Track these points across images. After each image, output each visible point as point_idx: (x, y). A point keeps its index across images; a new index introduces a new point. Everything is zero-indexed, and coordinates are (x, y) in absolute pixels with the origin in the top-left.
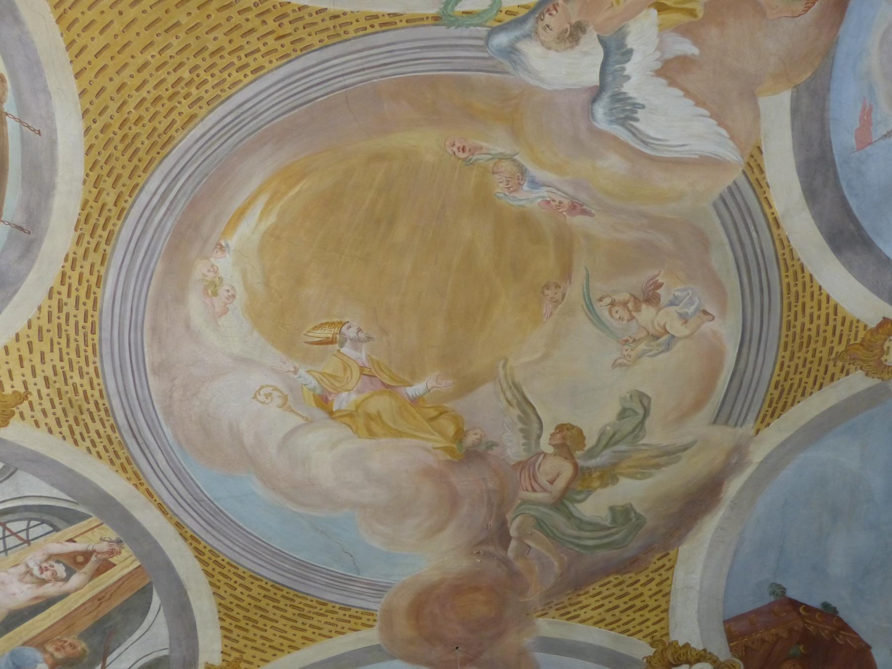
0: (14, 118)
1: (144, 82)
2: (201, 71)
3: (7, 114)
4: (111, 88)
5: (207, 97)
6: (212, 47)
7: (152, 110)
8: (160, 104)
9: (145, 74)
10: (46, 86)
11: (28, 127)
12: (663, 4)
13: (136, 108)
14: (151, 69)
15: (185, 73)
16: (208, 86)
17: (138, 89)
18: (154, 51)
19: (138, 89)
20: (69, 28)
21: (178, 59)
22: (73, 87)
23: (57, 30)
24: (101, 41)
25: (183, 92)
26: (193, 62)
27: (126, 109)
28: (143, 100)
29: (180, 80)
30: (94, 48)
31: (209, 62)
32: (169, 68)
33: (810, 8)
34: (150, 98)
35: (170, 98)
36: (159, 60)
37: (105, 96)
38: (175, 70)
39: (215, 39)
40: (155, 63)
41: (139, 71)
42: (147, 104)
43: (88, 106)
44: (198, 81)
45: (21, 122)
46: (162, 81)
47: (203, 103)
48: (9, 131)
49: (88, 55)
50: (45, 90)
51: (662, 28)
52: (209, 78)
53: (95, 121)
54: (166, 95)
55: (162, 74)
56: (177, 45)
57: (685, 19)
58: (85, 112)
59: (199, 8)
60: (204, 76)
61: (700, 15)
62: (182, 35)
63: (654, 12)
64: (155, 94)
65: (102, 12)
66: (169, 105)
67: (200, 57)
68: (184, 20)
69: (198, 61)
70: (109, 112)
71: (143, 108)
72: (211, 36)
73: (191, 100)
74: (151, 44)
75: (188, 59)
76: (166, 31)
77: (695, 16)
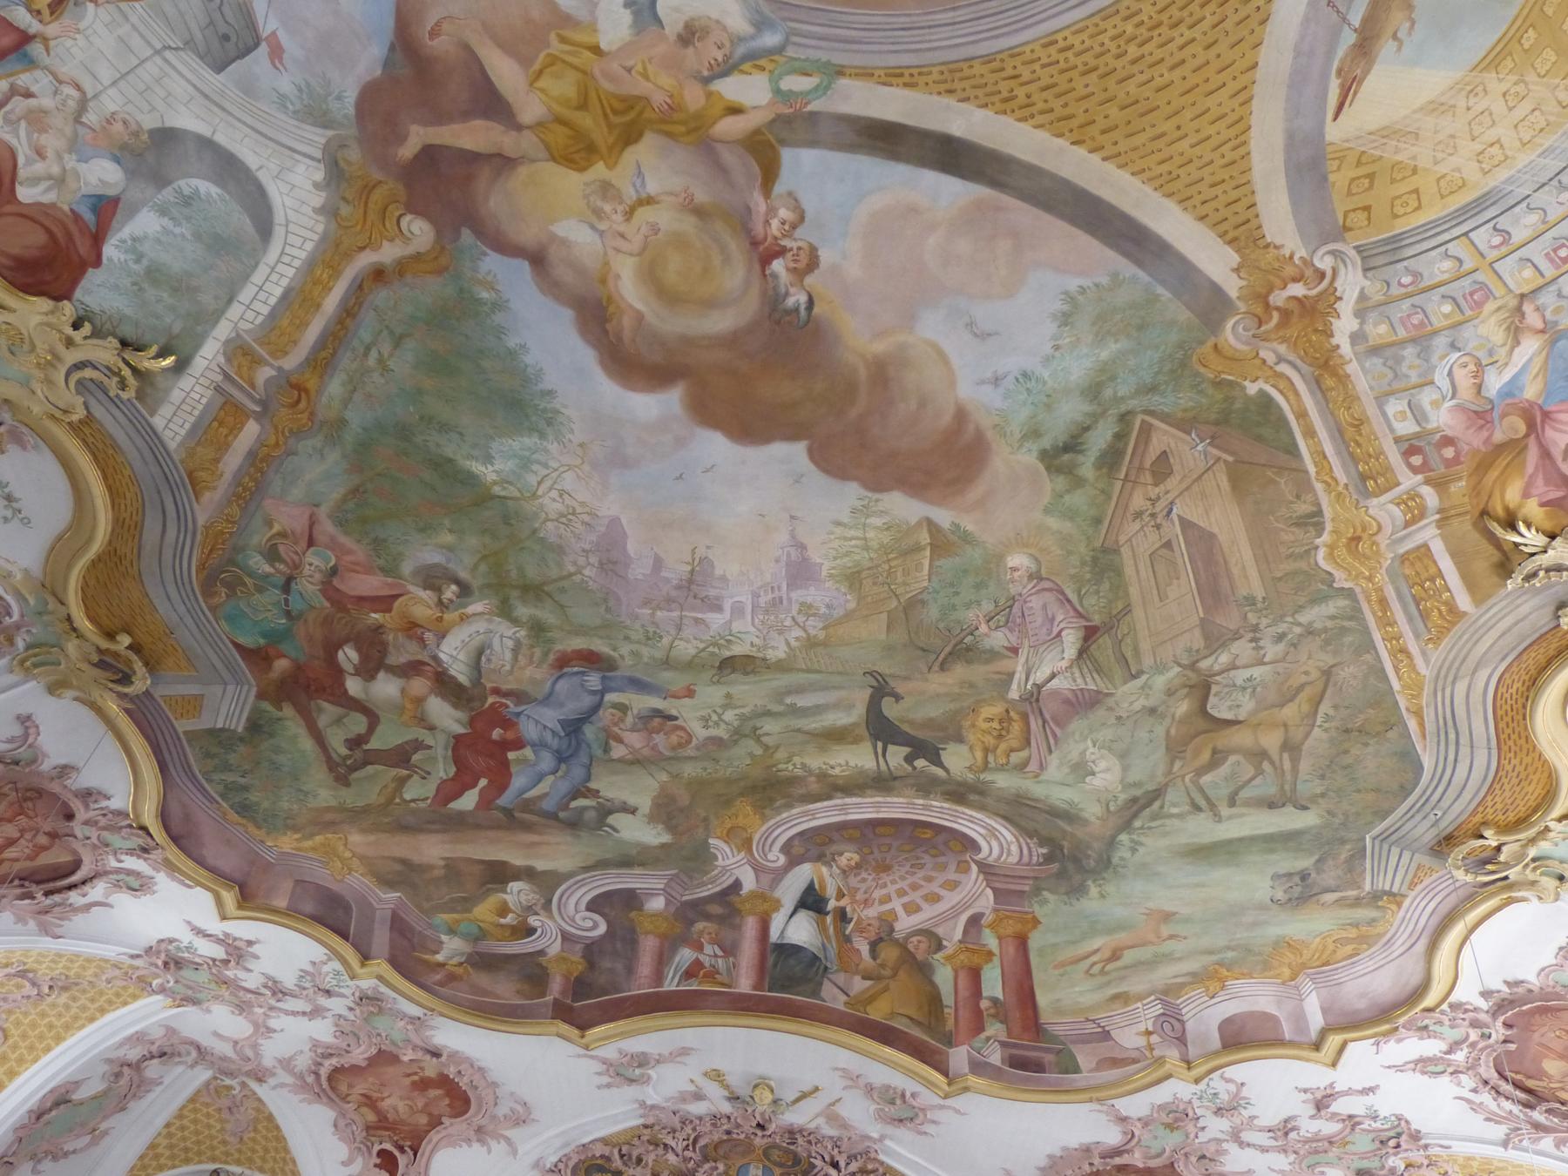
0: (1349, 24)
1: (1182, 48)
2: (1114, 51)
3: (1355, 30)
4: (1222, 47)
5: (1117, 20)
6: (1094, 76)
7: (1185, 13)
8: (1174, 20)
9: (1178, 56)
10: (1295, 58)
11: (1338, 12)
12: (595, 54)
13: (1204, 18)
14: (1170, 62)
15: (1133, 51)
16: (1112, 32)
17: (1194, 40)
18: (1159, 81)
19: (1194, 40)
20: (1242, 118)
21: (1135, 68)
22: (1265, 55)
23: (1254, 120)
24: (1211, 102)
25: (1143, 30)
26: (1119, 64)
27: (1216, 18)
28: (1191, 27)
29: (1141, 45)
30: (1223, 94)
31: (1102, 61)
32: (1149, 60)
33: (436, 24)
34: (1183, 28)
35: (1159, 24)
36: (1156, 71)
37: (1233, 39)
38: (1143, 56)
39: (1087, 86)
40: (1163, 68)
41: (1183, 61)
42: (1189, 21)
43: (1257, 29)
44: (1122, 42)
45: (1344, 19)
46: (1162, 46)
47: (1124, 13)
48: (1364, 9)
49: (1233, 87)
50: (1298, 53)
51: (593, 28)
52: (1107, 41)
53: (1258, 8)
54: (1163, 29)
55: (1159, 54)
56: (1131, 86)
57: (568, 33)
58: (1263, 22)
59: (1094, 121)
60: (1112, 46)
61: (553, 37)
62: (1122, 95)
63: (603, 46)
64: (1175, 33)
65: (1197, 131)
66: (1164, 17)
67: (1111, 67)
68: (1113, 111)
69: (1113, 63)
70: (1237, 18)
71: (1195, 18)
72: (1090, 89)
73: (1136, 19)
74: (1159, 90)
75: (1124, 68)
76: (1137, 102)
77: (559, 35)
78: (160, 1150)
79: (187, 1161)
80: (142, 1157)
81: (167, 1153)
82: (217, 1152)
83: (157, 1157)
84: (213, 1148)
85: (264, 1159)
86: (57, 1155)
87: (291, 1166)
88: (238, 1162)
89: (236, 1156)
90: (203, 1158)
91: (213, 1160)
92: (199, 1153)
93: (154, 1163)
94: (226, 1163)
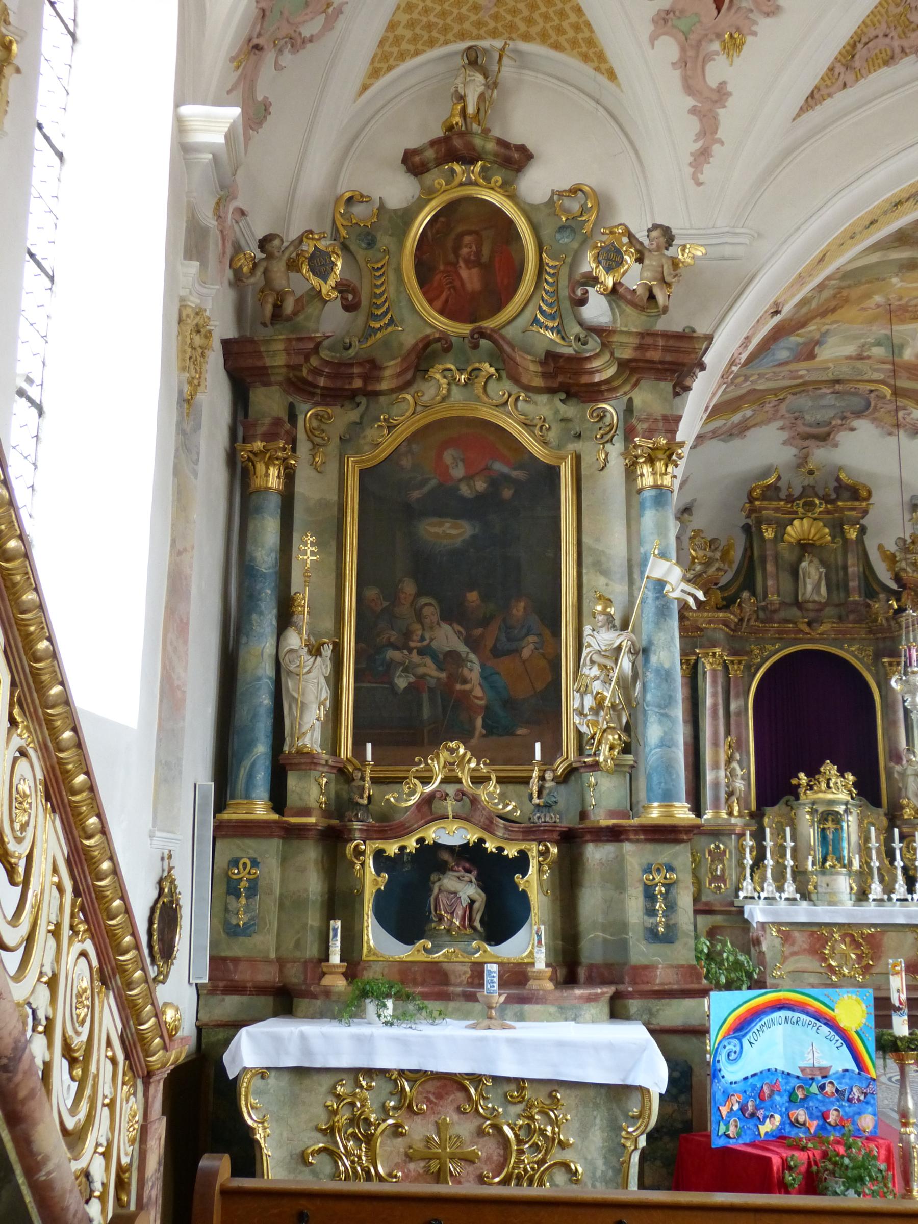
78: (400, 31)
79: (432, 43)
80: (381, 43)
81: (408, 34)
82: (467, 25)
83: (397, 41)
84: (461, 19)
85: (530, 21)
86: (296, 43)
87: (573, 18)
88: (494, 34)
89: (492, 24)
90: (450, 36)
91: (462, 36)
92: (445, 30)
93: (395, 50)
94: (479, 37)
